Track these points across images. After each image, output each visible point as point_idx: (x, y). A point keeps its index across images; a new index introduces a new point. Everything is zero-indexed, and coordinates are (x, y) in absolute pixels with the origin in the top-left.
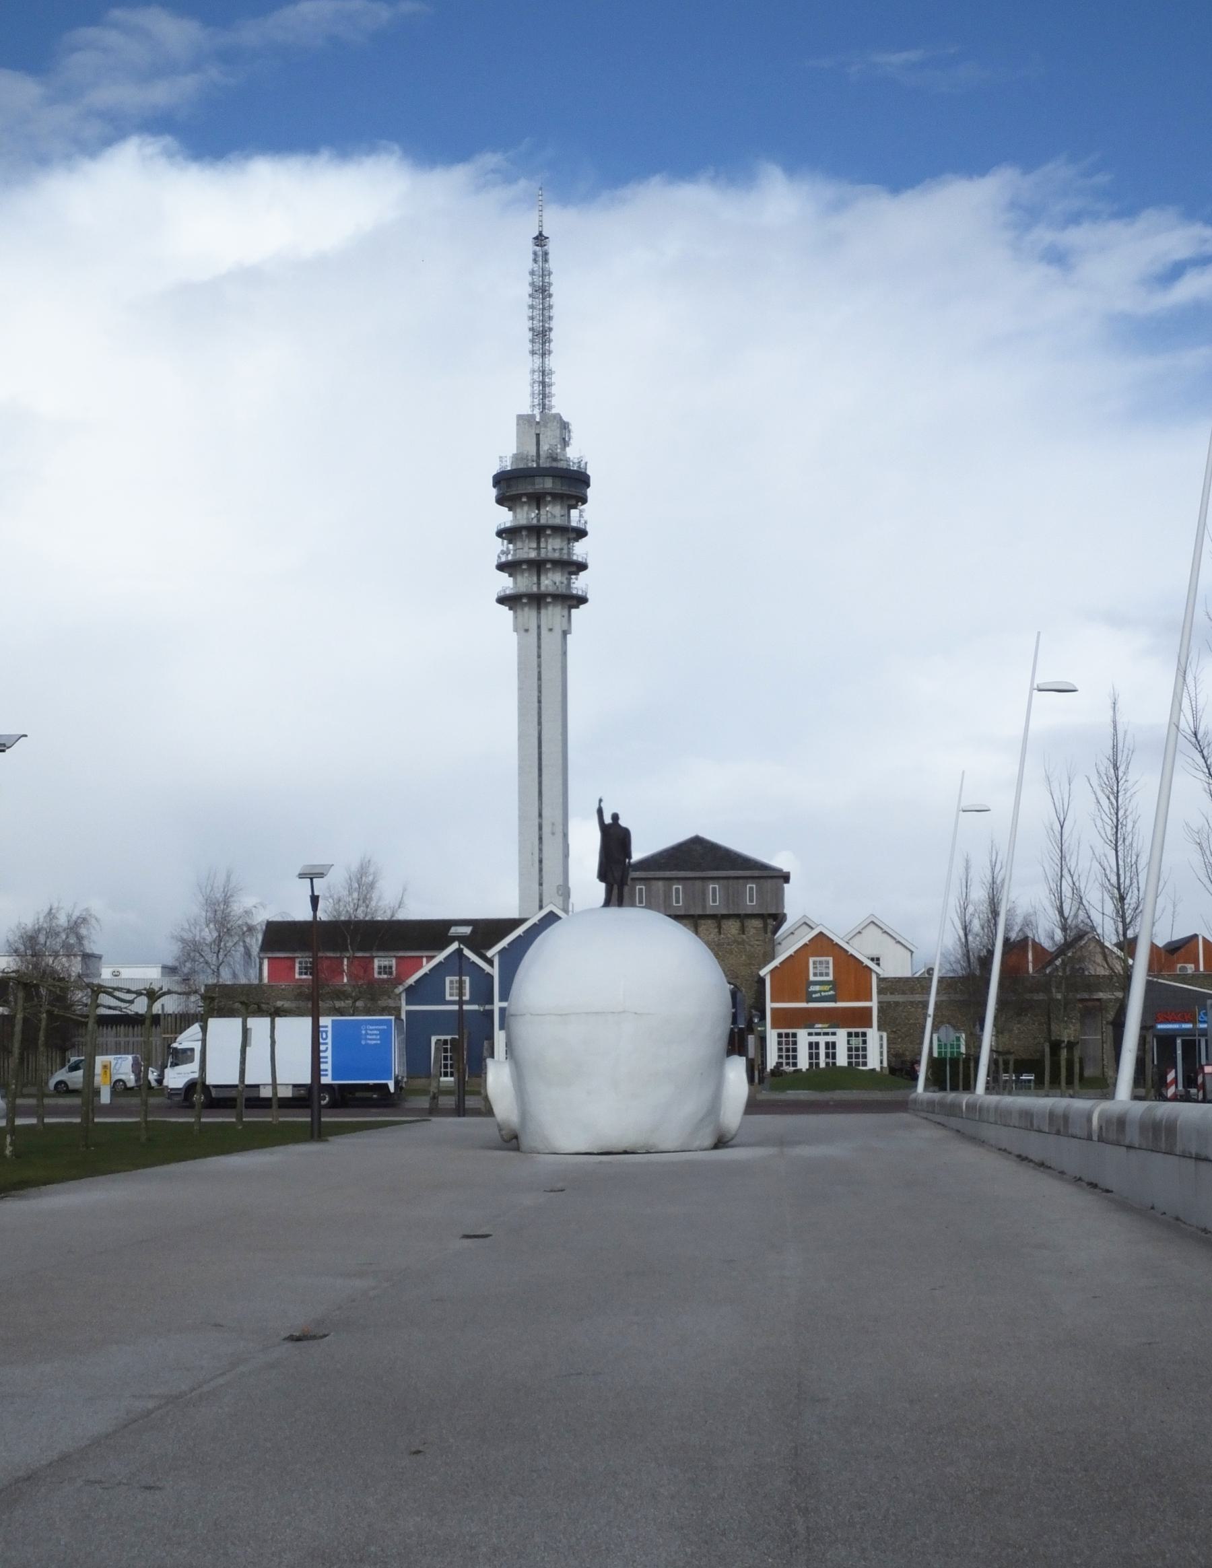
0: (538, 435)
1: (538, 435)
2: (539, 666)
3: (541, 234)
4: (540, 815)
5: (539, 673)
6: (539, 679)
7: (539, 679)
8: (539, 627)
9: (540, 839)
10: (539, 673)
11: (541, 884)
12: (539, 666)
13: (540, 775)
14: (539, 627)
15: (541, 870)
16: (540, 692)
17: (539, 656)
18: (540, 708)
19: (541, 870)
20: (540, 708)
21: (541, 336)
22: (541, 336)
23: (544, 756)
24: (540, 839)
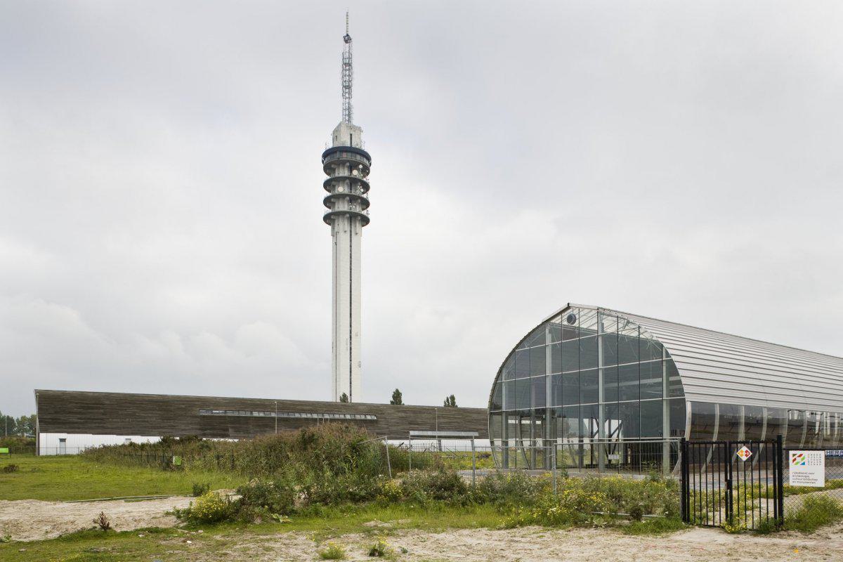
0: (351, 135)
1: (351, 135)
2: (351, 251)
3: (348, 35)
4: (351, 326)
5: (351, 254)
6: (351, 257)
7: (351, 257)
8: (351, 231)
9: (351, 337)
10: (351, 254)
11: (351, 360)
12: (351, 251)
13: (351, 306)
14: (351, 231)
15: (351, 353)
16: (351, 264)
17: (351, 246)
18: (351, 272)
19: (351, 353)
20: (351, 272)
21: (347, 87)
22: (347, 87)
23: (352, 297)
24: (351, 337)
